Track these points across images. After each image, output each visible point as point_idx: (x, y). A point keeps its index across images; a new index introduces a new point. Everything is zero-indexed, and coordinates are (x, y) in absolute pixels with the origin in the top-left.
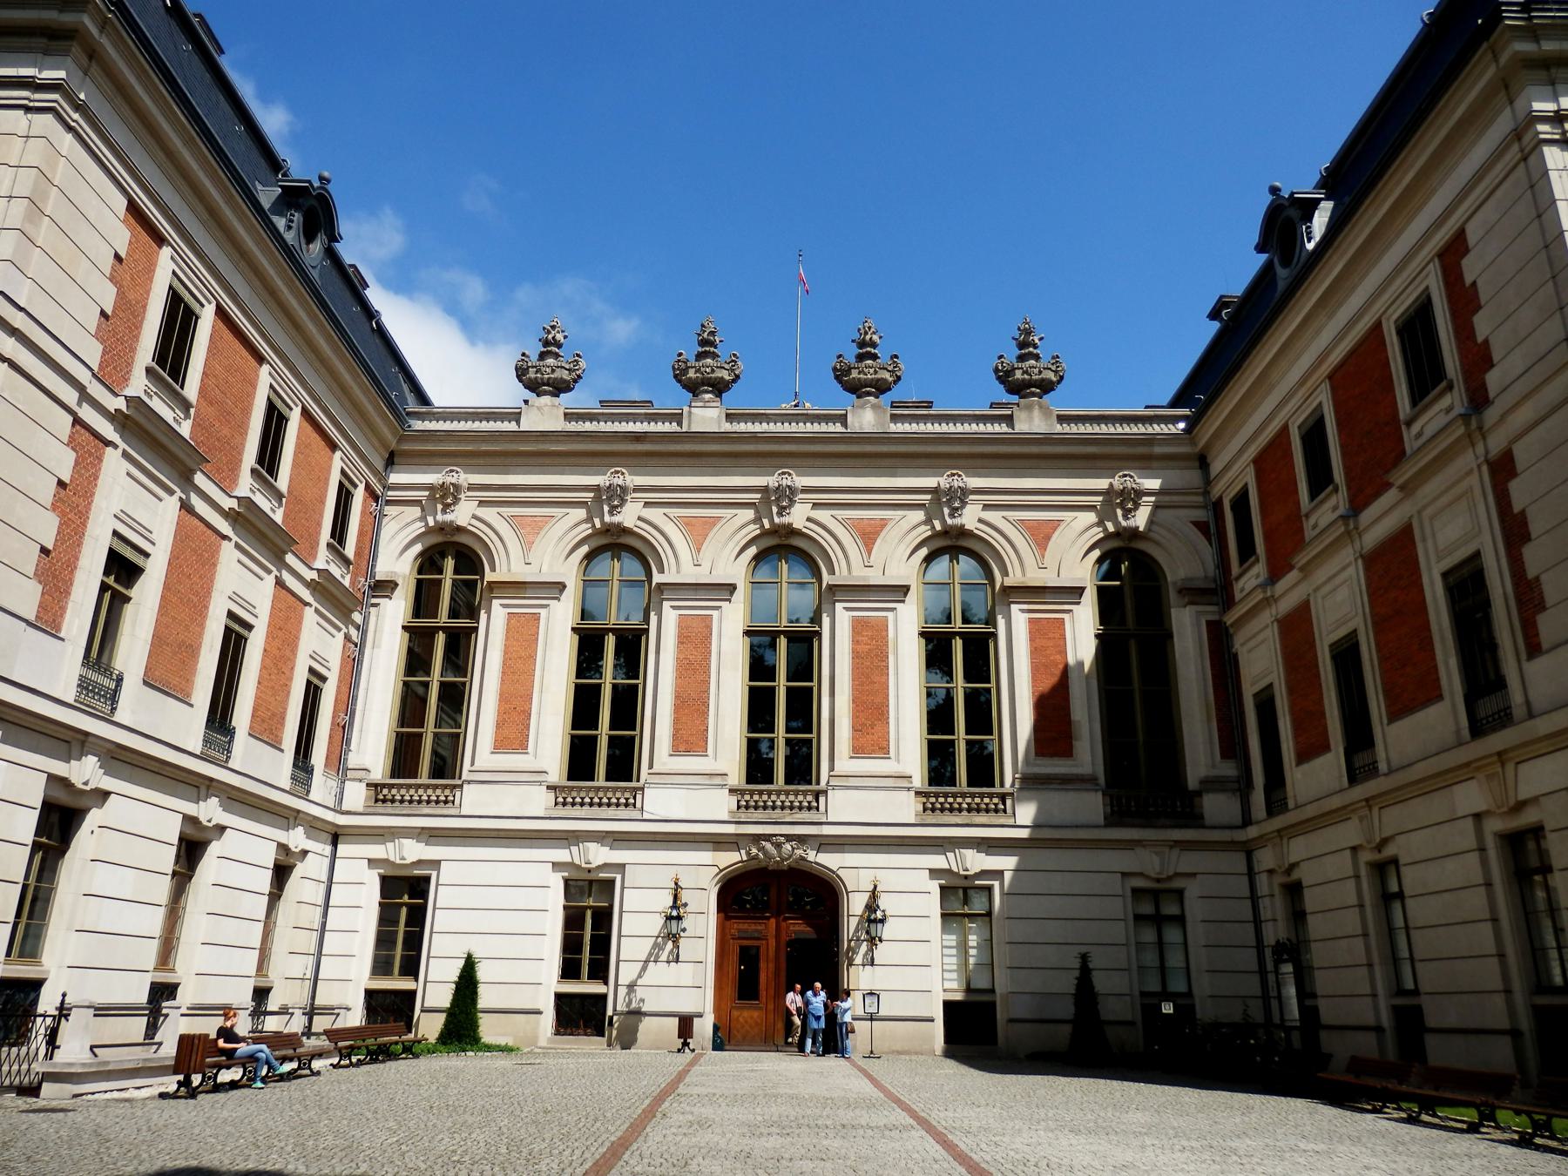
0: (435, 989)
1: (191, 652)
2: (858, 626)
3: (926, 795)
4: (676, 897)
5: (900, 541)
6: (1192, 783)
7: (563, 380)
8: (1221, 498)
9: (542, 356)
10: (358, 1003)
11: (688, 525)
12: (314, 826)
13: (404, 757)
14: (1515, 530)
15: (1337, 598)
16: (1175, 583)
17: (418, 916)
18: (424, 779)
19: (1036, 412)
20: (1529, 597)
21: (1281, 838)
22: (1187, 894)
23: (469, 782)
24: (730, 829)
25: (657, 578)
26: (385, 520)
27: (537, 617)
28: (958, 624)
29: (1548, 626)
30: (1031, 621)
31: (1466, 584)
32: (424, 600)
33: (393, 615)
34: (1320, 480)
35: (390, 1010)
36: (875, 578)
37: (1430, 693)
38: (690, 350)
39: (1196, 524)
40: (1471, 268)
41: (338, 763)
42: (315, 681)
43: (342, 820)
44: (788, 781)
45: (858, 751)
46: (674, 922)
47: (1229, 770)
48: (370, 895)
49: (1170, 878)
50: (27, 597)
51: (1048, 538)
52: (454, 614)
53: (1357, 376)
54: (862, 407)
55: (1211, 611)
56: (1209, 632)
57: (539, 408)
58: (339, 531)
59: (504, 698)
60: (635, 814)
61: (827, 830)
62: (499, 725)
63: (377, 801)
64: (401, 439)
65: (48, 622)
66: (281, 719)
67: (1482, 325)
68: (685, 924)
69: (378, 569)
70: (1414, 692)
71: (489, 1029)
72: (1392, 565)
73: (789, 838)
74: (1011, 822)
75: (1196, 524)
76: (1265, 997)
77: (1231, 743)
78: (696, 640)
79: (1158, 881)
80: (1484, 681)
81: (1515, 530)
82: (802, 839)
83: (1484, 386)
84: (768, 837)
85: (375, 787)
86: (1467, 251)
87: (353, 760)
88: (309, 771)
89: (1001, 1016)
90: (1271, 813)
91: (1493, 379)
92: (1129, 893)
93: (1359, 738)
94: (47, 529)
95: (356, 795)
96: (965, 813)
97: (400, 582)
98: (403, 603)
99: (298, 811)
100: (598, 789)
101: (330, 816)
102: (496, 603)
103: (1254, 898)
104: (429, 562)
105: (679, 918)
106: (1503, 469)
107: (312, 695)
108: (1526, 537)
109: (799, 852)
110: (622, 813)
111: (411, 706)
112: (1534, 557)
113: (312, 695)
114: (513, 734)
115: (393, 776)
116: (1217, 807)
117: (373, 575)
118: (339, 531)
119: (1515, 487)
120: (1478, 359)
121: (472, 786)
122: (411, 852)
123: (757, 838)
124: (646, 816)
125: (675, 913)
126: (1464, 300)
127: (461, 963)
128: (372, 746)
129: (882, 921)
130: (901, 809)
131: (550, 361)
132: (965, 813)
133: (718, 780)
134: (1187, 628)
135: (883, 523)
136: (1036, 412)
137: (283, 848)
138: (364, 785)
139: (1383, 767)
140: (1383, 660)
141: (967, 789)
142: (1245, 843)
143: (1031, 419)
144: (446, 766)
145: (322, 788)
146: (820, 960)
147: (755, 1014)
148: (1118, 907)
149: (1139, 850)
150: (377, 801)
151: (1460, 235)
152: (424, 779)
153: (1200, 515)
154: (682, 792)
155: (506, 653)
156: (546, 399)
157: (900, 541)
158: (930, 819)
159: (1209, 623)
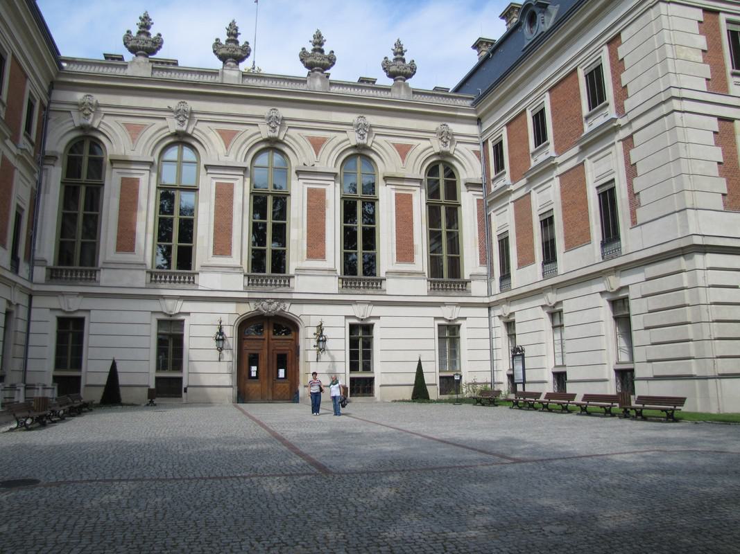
0: (93, 372)
2: (311, 192)
3: (343, 279)
4: (220, 329)
5: (333, 150)
6: (466, 277)
7: (151, 49)
8: (487, 140)
9: (139, 33)
10: (49, 381)
11: (221, 133)
12: (23, 289)
13: (64, 254)
16: (464, 180)
17: (79, 339)
19: (403, 88)
21: (507, 301)
22: (461, 327)
23: (103, 268)
24: (245, 295)
25: (204, 162)
26: (49, 121)
28: (359, 194)
29: (641, 215)
30: (396, 194)
32: (72, 168)
33: (55, 175)
34: (541, 137)
35: (68, 385)
37: (585, 239)
38: (224, 38)
39: (475, 152)
40: (622, 51)
42: (19, 211)
43: (35, 288)
44: (273, 271)
46: (221, 342)
47: (484, 270)
48: (52, 328)
49: (455, 320)
51: (406, 153)
52: (89, 175)
54: (315, 77)
55: (480, 194)
56: (478, 205)
57: (138, 63)
58: (28, 128)
60: (194, 287)
61: (295, 296)
62: (119, 238)
63: (51, 277)
64: (58, 74)
68: (226, 342)
69: (46, 149)
70: (578, 238)
71: (125, 395)
73: (276, 300)
74: (384, 293)
75: (475, 152)
76: (492, 371)
77: (485, 258)
78: (224, 195)
79: (450, 321)
80: (611, 234)
81: (631, 170)
83: (623, 106)
84: (264, 299)
86: (621, 44)
87: (37, 255)
89: (377, 383)
90: (502, 290)
91: (628, 104)
92: (436, 327)
93: (550, 255)
95: (40, 273)
96: (362, 288)
97: (59, 157)
98: (60, 169)
99: (16, 283)
100: (174, 273)
101: (28, 285)
102: (114, 170)
103: (490, 328)
104: (75, 147)
105: (223, 340)
106: (628, 142)
108: (635, 175)
109: (282, 307)
110: (187, 286)
111: (65, 228)
112: (638, 184)
115: (59, 264)
116: (478, 289)
117: (44, 152)
118: (28, 128)
119: (632, 152)
120: (622, 93)
121: (106, 270)
122: (73, 305)
124: (200, 288)
125: (221, 337)
127: (111, 362)
128: (47, 247)
129: (324, 341)
130: (332, 285)
131: (143, 36)
132: (362, 288)
133: (238, 270)
134: (468, 203)
136: (403, 88)
137: (9, 303)
138: (44, 269)
140: (565, 223)
141: (363, 277)
142: (488, 303)
143: (400, 92)
146: (287, 359)
147: (258, 386)
148: (434, 333)
149: (443, 308)
150: (51, 277)
151: (618, 36)
153: (478, 148)
154: (219, 275)
155: (121, 199)
156: (141, 59)
157: (333, 150)
158: (345, 290)
159: (478, 200)
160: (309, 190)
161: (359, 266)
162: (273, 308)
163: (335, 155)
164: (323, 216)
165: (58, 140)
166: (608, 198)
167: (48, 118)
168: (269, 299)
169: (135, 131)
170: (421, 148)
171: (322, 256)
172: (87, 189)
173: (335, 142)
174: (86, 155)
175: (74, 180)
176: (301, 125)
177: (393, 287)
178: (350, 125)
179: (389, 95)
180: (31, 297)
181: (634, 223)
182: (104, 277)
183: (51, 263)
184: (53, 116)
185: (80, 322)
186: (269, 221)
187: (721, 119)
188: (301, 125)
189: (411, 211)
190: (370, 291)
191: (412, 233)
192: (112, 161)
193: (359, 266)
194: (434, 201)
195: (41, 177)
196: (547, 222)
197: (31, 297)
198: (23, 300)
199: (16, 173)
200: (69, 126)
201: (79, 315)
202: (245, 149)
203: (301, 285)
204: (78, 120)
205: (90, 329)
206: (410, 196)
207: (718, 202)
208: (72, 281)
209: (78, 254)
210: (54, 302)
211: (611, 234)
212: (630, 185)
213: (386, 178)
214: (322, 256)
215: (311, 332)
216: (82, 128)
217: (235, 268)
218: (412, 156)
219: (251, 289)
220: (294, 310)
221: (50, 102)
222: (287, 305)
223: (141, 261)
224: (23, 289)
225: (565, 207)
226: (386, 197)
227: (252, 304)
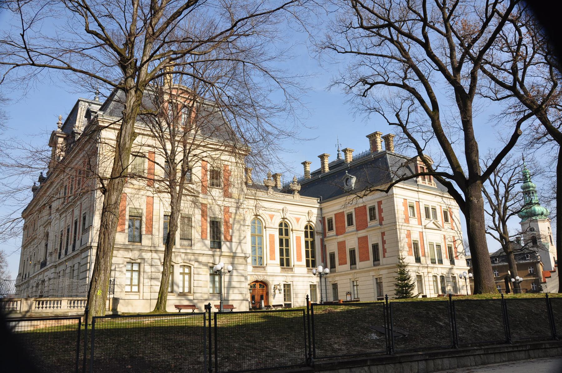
2: (270, 235)
14: (384, 242)
15: (352, 242)
20: (384, 251)
24: (253, 273)
29: (386, 255)
31: (375, 247)
37: (368, 259)
40: (382, 206)
45: (271, 259)
53: (360, 211)
67: (383, 215)
72: (363, 241)
80: (376, 259)
81: (384, 242)
106: (383, 234)
120: (381, 219)
126: (381, 211)
139: (357, 268)
161: (285, 263)
166: (375, 247)
168: (260, 275)
177: (296, 270)
181: (384, 257)
193: (285, 263)
194: (307, 239)
196: (352, 252)
203: (269, 269)
211: (376, 259)
212: (383, 247)
215: (273, 287)
225: (359, 248)
227: (255, 276)
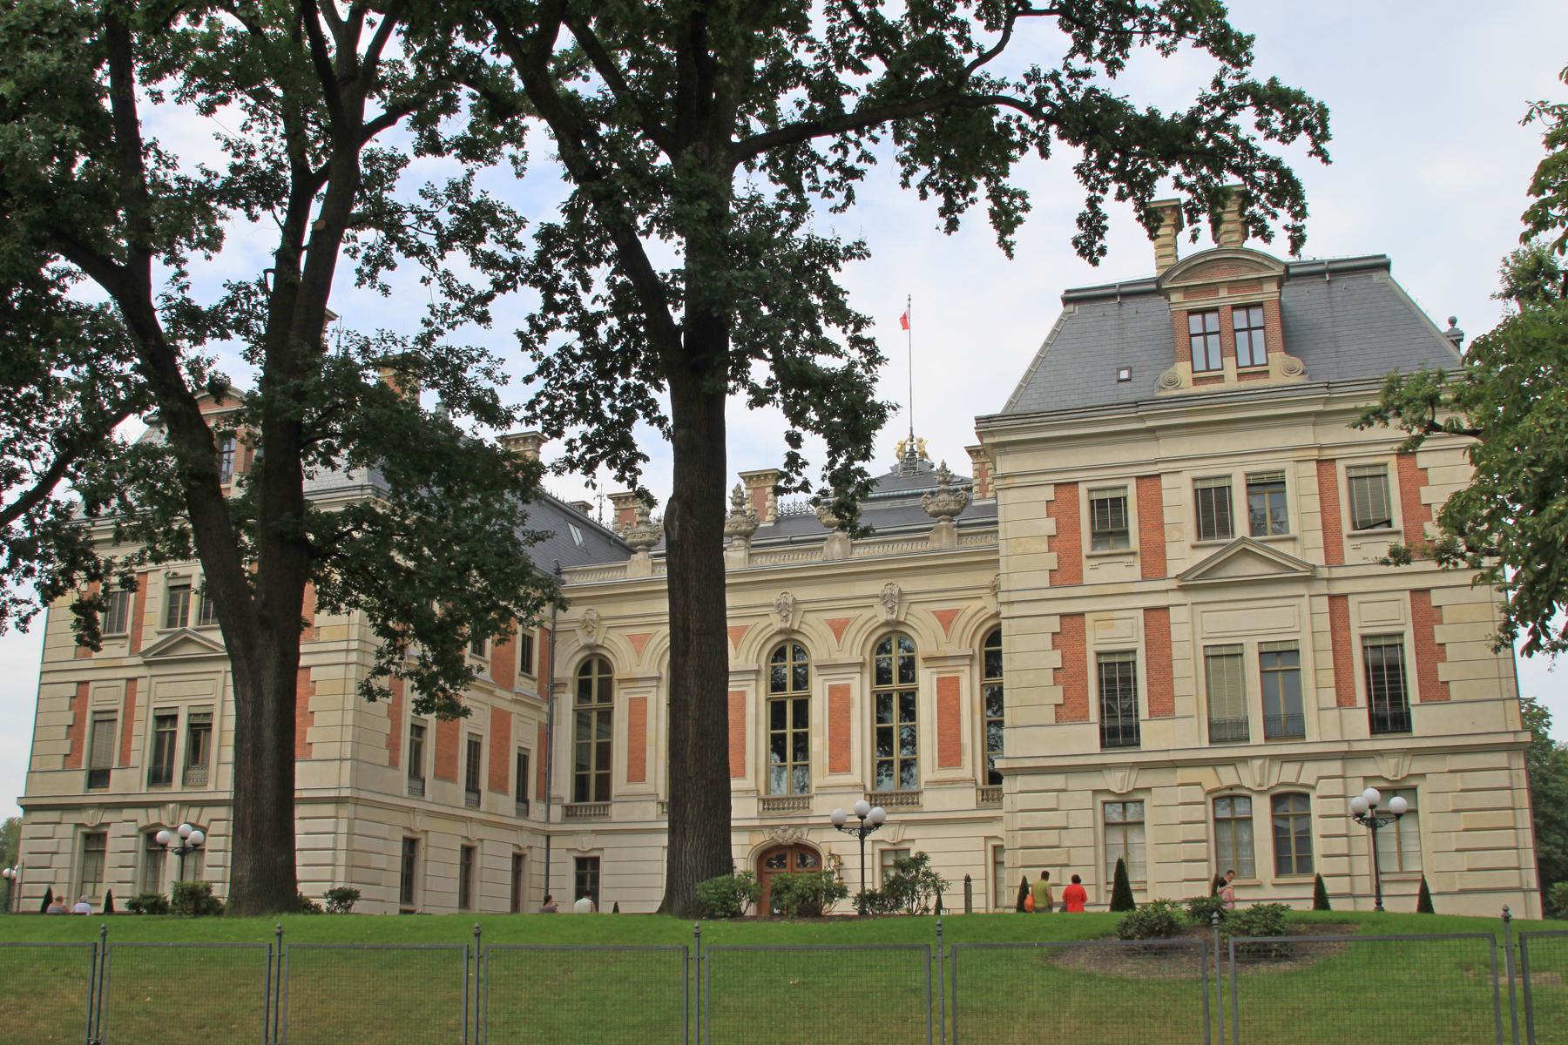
1: (453, 759)
2: (833, 690)
18: (592, 802)
24: (757, 823)
27: (645, 699)
32: (584, 690)
33: (567, 701)
36: (842, 658)
41: (545, 795)
45: (833, 770)
50: (384, 756)
51: (950, 622)
59: (631, 751)
61: (811, 821)
65: (394, 763)
66: (506, 779)
73: (791, 826)
82: (799, 826)
85: (568, 808)
87: (554, 793)
88: (527, 802)
94: (387, 726)
95: (556, 812)
104: (585, 668)
107: (523, 760)
113: (523, 760)
114: (637, 773)
118: (526, 666)
122: (587, 845)
123: (772, 827)
128: (563, 785)
135: (846, 622)
143: (940, 539)
144: (604, 792)
145: (537, 809)
152: (592, 802)
160: (831, 687)
162: (788, 837)
163: (861, 638)
164: (848, 719)
165: (566, 669)
167: (554, 642)
169: (639, 642)
170: (970, 612)
171: (847, 769)
172: (599, 714)
173: (861, 621)
174: (595, 677)
175: (585, 706)
176: (818, 607)
177: (932, 802)
178: (877, 596)
179: (929, 546)
180: (548, 838)
182: (616, 810)
183: (567, 800)
184: (559, 637)
185: (596, 861)
186: (789, 731)
187: (1062, 616)
188: (818, 607)
189: (958, 699)
190: (902, 808)
191: (959, 729)
192: (620, 681)
195: (551, 709)
197: (548, 838)
198: (542, 841)
199: (514, 718)
200: (576, 647)
201: (594, 854)
202: (756, 646)
204: (583, 639)
205: (604, 868)
206: (957, 679)
207: (1049, 715)
208: (586, 818)
209: (593, 787)
210: (570, 842)
213: (925, 659)
214: (847, 769)
216: (587, 647)
217: (748, 791)
218: (959, 624)
219: (766, 814)
220: (812, 838)
221: (554, 624)
222: (805, 830)
223: (652, 790)
224: (534, 831)
226: (926, 683)
227: (766, 831)
